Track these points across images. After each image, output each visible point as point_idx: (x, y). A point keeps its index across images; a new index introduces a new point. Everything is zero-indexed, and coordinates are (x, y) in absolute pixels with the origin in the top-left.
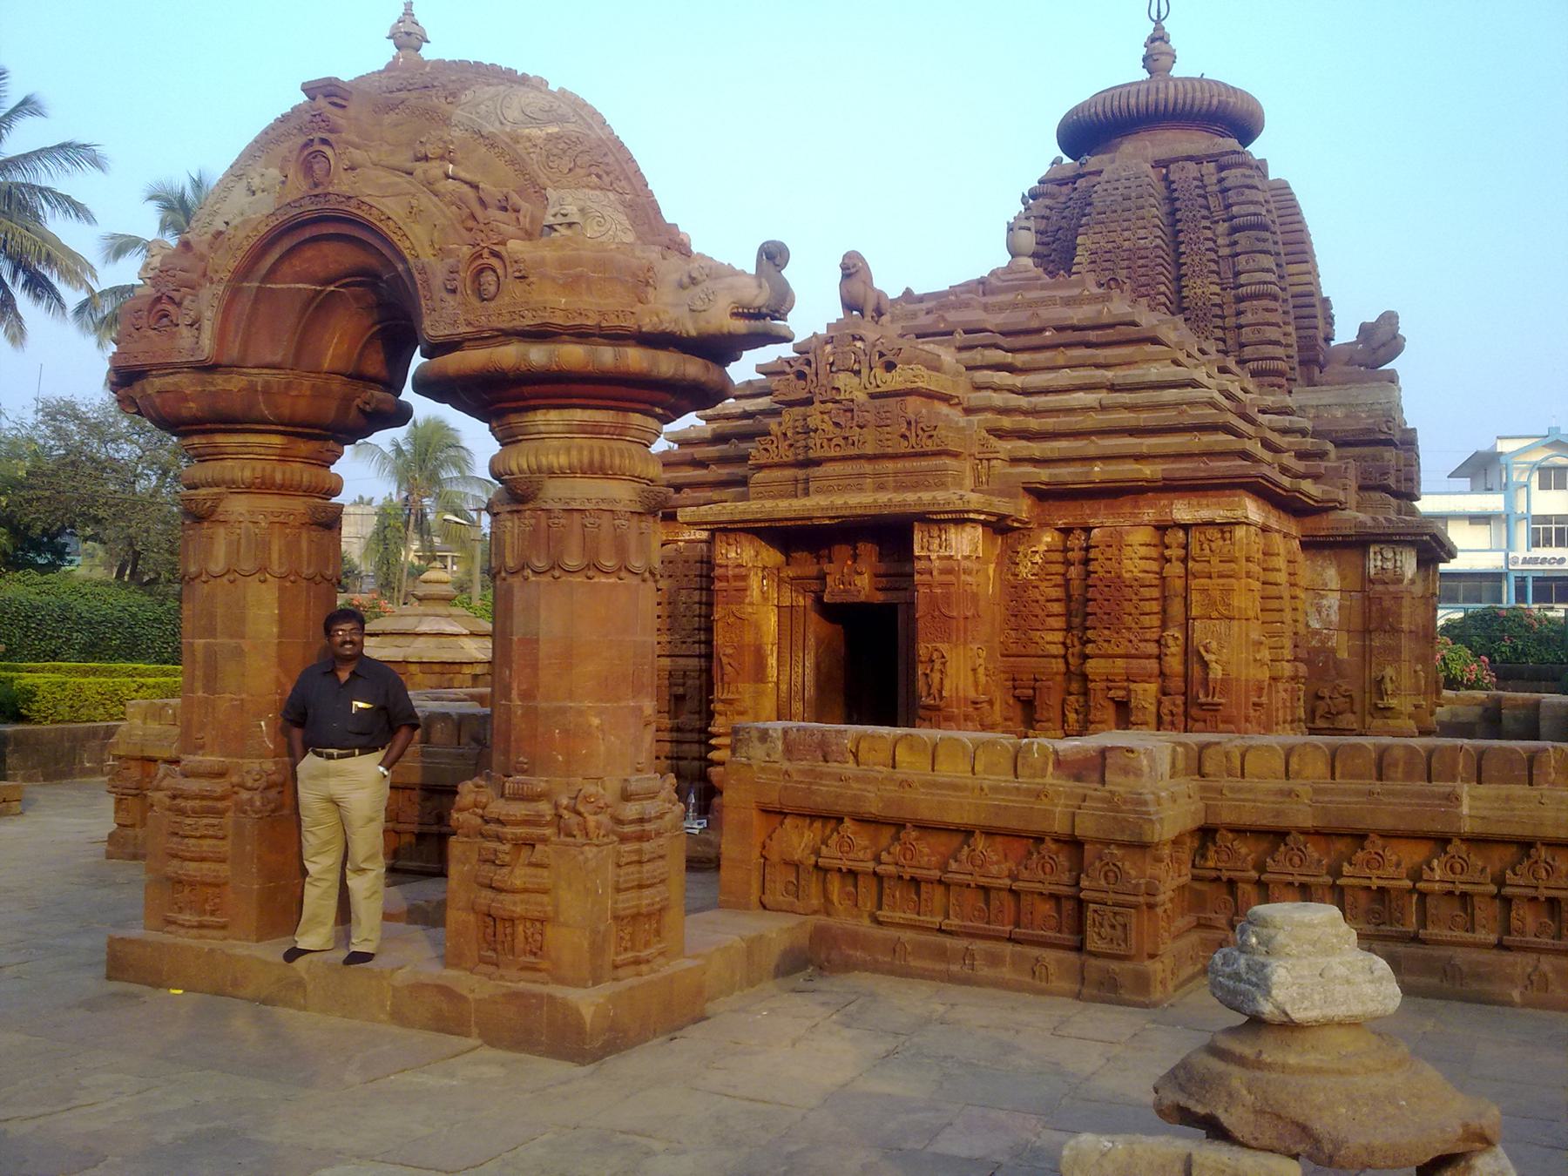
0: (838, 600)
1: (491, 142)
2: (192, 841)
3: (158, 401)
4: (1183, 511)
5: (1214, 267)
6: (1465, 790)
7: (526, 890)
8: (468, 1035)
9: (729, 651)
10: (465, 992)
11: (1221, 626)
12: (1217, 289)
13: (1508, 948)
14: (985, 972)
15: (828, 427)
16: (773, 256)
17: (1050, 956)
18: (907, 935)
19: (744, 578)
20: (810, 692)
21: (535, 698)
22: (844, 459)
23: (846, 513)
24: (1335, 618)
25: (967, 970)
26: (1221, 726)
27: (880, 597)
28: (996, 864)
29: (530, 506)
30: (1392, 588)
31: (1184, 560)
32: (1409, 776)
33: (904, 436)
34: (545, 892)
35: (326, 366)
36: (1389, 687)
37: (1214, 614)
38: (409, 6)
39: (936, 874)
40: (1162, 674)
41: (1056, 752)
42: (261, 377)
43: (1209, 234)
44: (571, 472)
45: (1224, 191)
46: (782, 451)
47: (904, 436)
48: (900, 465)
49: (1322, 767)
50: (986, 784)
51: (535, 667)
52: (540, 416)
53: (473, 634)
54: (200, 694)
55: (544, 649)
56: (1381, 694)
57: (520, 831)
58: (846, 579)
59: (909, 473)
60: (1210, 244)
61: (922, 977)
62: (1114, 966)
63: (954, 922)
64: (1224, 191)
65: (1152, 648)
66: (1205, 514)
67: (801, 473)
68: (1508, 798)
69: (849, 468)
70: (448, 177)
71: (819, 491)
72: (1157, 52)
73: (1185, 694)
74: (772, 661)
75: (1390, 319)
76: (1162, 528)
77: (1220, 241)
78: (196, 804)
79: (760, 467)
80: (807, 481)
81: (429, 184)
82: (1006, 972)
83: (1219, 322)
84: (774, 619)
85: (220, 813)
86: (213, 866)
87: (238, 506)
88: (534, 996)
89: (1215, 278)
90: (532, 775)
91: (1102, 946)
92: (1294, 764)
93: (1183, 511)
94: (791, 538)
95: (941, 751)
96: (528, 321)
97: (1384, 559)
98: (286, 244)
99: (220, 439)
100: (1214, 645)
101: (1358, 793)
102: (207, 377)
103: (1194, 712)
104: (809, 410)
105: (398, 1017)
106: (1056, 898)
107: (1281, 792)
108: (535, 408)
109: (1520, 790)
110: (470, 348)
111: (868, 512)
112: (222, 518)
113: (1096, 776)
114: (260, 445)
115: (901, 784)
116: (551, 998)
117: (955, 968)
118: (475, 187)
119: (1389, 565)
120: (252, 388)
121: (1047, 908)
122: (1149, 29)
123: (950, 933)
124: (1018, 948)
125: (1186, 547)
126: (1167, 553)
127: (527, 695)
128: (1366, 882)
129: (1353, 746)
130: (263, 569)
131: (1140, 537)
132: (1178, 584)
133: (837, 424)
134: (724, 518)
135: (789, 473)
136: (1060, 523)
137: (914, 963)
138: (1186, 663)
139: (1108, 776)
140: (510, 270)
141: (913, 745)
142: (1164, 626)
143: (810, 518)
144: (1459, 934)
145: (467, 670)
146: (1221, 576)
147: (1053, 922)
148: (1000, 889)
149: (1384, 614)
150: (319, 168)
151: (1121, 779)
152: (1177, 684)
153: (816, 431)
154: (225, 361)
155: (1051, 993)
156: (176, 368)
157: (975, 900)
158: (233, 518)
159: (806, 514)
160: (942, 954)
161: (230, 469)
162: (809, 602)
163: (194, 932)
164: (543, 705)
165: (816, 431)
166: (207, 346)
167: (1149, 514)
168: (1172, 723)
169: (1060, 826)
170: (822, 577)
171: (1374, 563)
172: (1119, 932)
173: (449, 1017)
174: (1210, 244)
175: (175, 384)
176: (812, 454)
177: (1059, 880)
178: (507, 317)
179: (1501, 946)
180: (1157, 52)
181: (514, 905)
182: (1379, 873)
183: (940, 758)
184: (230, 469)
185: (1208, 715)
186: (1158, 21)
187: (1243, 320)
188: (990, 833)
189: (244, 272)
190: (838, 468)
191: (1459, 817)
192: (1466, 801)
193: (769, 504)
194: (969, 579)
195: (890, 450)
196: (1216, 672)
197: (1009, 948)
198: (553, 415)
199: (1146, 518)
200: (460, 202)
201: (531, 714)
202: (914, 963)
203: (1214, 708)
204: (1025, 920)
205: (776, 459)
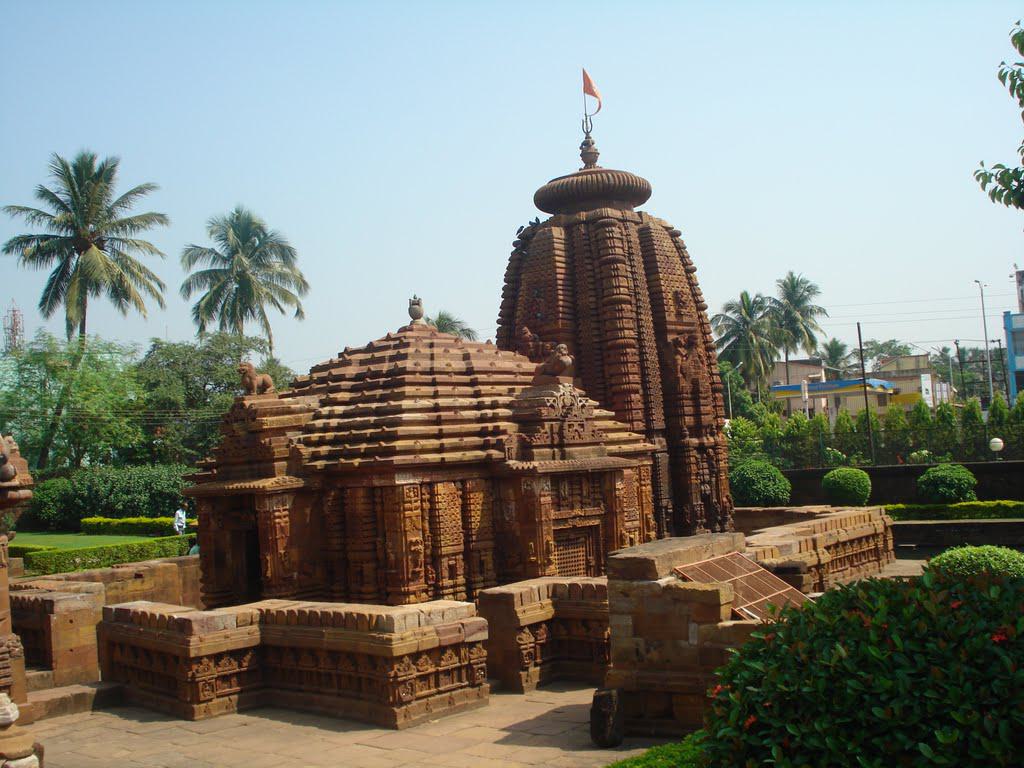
5: (591, 287)
12: (592, 299)
24: (514, 515)
43: (589, 267)
45: (597, 241)
60: (591, 273)
64: (597, 241)
72: (588, 153)
74: (229, 556)
77: (597, 270)
83: (595, 319)
84: (228, 537)
89: (593, 293)
93: (377, 483)
100: (390, 544)
119: (529, 488)
122: (583, 138)
131: (361, 493)
136: (339, 486)
174: (591, 273)
180: (588, 153)
186: (587, 133)
187: (605, 317)
194: (277, 520)
196: (392, 557)
199: (364, 484)
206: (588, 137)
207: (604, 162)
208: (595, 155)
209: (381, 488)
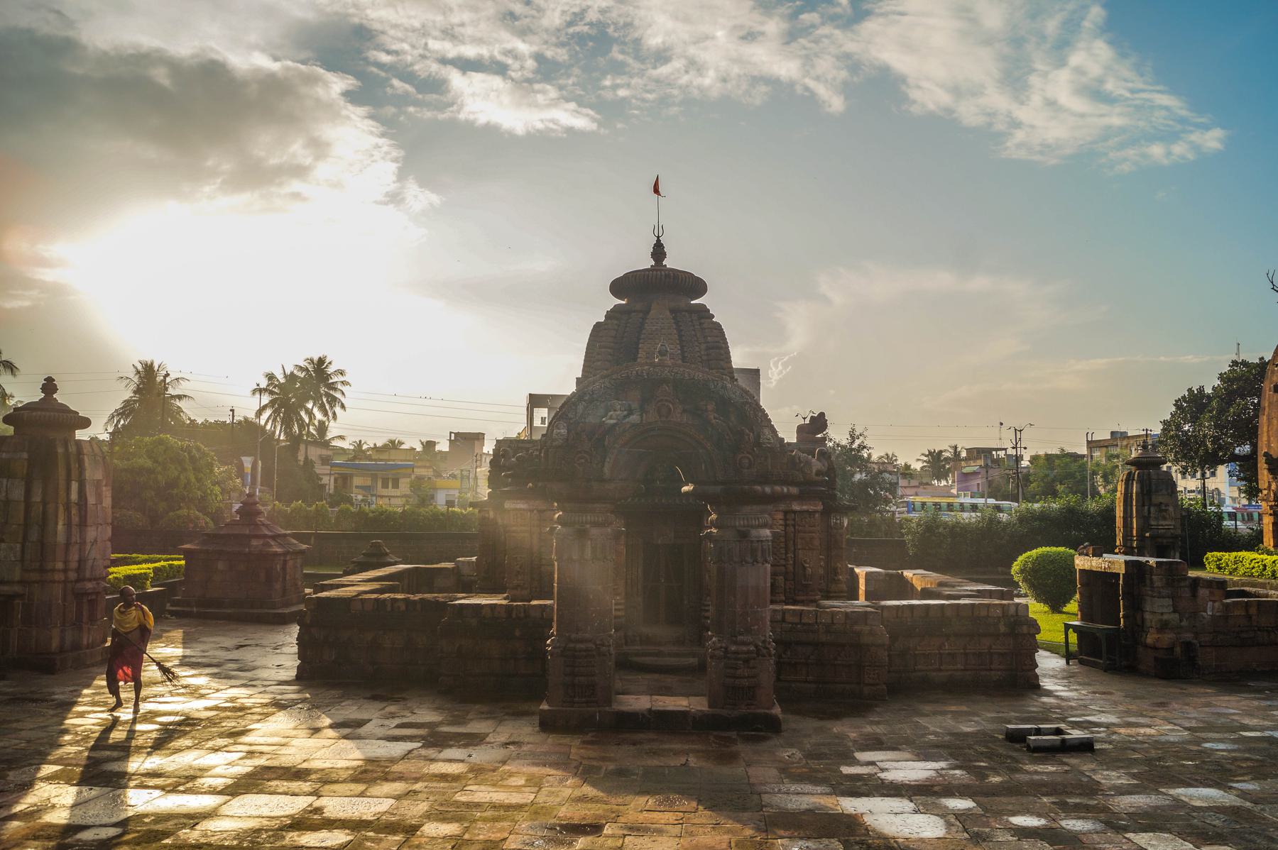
66: (805, 508)
72: (659, 252)
75: (822, 415)
76: (786, 513)
93: (796, 507)
131: (780, 516)
167: (782, 507)
180: (659, 252)
181: (745, 682)
206: (658, 240)
207: (669, 263)
208: (664, 255)
209: (801, 512)
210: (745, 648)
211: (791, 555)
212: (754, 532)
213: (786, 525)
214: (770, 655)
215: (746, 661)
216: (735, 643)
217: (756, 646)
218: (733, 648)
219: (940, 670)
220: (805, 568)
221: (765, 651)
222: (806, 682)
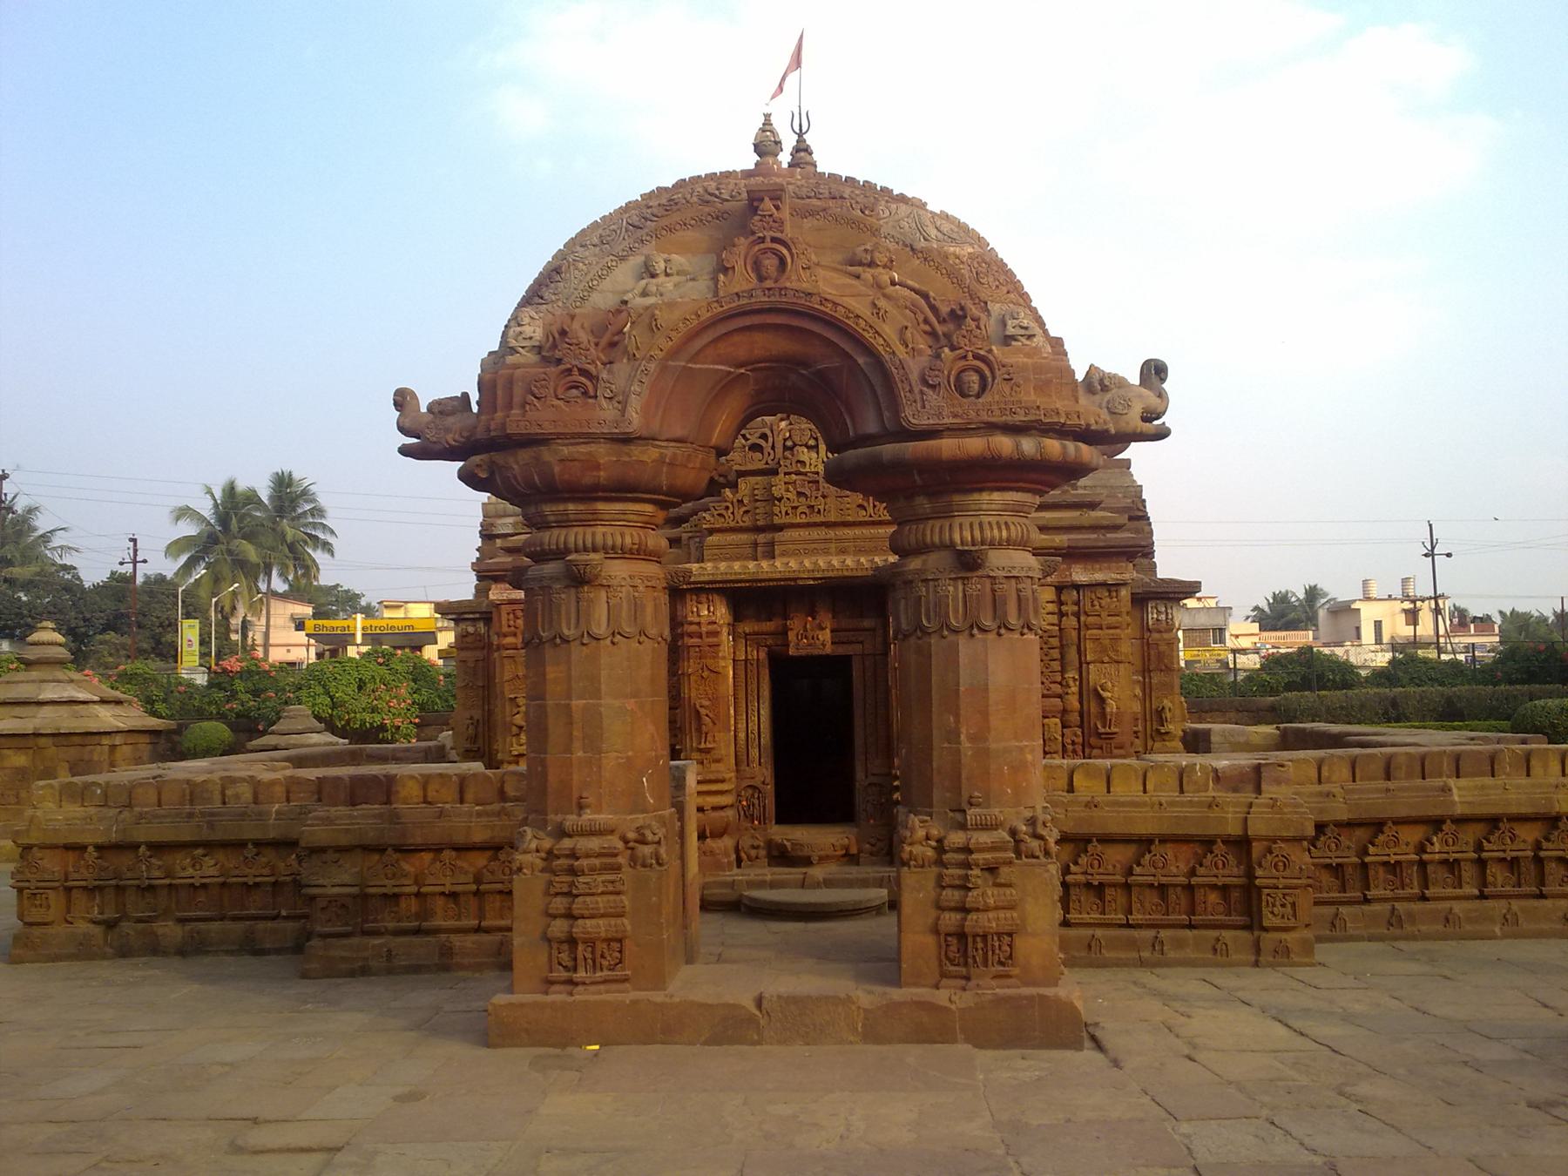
0: (803, 652)
1: (926, 256)
2: (588, 899)
3: (557, 469)
4: (1080, 575)
6: (1452, 782)
7: (996, 908)
8: (954, 1041)
9: (707, 703)
10: (947, 1004)
11: (1112, 668)
13: (1486, 898)
14: (1171, 954)
15: (792, 496)
16: (1155, 371)
17: (1227, 935)
18: (1099, 932)
19: (716, 634)
20: (766, 738)
21: (986, 739)
22: (809, 525)
23: (830, 574)
25: (1157, 955)
26: (1116, 752)
27: (842, 650)
28: (1175, 865)
29: (980, 573)
30: (1165, 636)
31: (1077, 615)
32: (1409, 776)
33: (861, 506)
34: (1012, 908)
35: (713, 442)
36: (1169, 715)
37: (1106, 659)
38: (767, 116)
39: (1119, 878)
40: (1065, 711)
41: (1216, 771)
42: (671, 450)
44: (1010, 543)
46: (738, 517)
47: (861, 506)
48: (857, 531)
49: (1345, 772)
50: (1163, 800)
51: (985, 714)
52: (985, 496)
53: (103, 702)
54: (580, 754)
55: (993, 696)
56: (1162, 722)
57: (988, 856)
58: (810, 634)
59: (865, 539)
61: (1117, 965)
62: (1284, 936)
63: (1136, 917)
65: (1057, 689)
66: (1099, 577)
67: (761, 538)
68: (1483, 787)
69: (816, 533)
70: (893, 283)
71: (783, 554)
73: (1081, 726)
76: (1060, 589)
78: (597, 862)
79: (711, 532)
80: (772, 544)
81: (879, 286)
82: (1189, 953)
85: (617, 868)
86: (613, 921)
87: (618, 570)
88: (1026, 998)
90: (988, 807)
91: (1277, 922)
92: (1325, 773)
93: (1080, 575)
94: (747, 600)
95: (1114, 775)
96: (1020, 417)
97: (1159, 612)
98: (722, 329)
99: (601, 506)
101: (1378, 790)
102: (625, 448)
103: (1093, 741)
104: (775, 480)
105: (872, 1035)
106: (1224, 889)
107: (1320, 794)
108: (981, 490)
109: (1488, 781)
110: (950, 437)
111: (855, 574)
112: (605, 582)
113: (1250, 787)
114: (638, 513)
115: (1087, 805)
116: (1042, 997)
117: (1146, 954)
118: (925, 296)
120: (661, 461)
121: (1213, 897)
123: (1139, 926)
124: (1195, 932)
125: (1077, 603)
126: (1064, 608)
127: (979, 737)
128: (1385, 858)
129: (1368, 755)
130: (642, 632)
132: (1074, 634)
133: (800, 494)
134: (706, 578)
135: (744, 537)
137: (1107, 954)
138: (1081, 703)
139: (1264, 787)
140: (998, 373)
141: (1090, 773)
142: (1063, 672)
143: (795, 579)
144: (1450, 891)
145: (106, 741)
146: (1109, 628)
147: (1221, 909)
148: (1176, 886)
149: (1160, 656)
150: (770, 263)
151: (1274, 788)
152: (1074, 718)
153: (780, 500)
154: (645, 433)
155: (1231, 965)
156: (590, 438)
157: (1152, 898)
158: (614, 582)
159: (792, 575)
160: (1133, 944)
161: (600, 533)
162: (763, 655)
163: (602, 987)
164: (993, 746)
165: (780, 500)
166: (635, 420)
168: (1074, 751)
169: (1234, 829)
170: (784, 632)
171: (1152, 616)
172: (1289, 909)
173: (932, 1029)
175: (590, 453)
176: (777, 520)
177: (1231, 873)
178: (998, 413)
179: (1482, 896)
181: (988, 922)
182: (1396, 850)
183: (1115, 781)
184: (600, 533)
185: (1104, 743)
186: (800, 134)
188: (1164, 840)
189: (674, 353)
190: (803, 533)
191: (1453, 803)
192: (1455, 791)
193: (723, 566)
195: (850, 519)
196: (1111, 707)
197: (1188, 933)
198: (996, 496)
200: (914, 308)
201: (983, 754)
202: (1107, 954)
203: (1110, 736)
204: (1199, 909)
205: (732, 524)
210: (984, 838)
211: (1072, 674)
212: (1000, 561)
213: (1061, 614)
214: (1047, 853)
215: (992, 870)
216: (963, 826)
217: (1013, 832)
218: (956, 838)
219: (1424, 898)
220: (1102, 701)
221: (1035, 844)
222: (1128, 926)
